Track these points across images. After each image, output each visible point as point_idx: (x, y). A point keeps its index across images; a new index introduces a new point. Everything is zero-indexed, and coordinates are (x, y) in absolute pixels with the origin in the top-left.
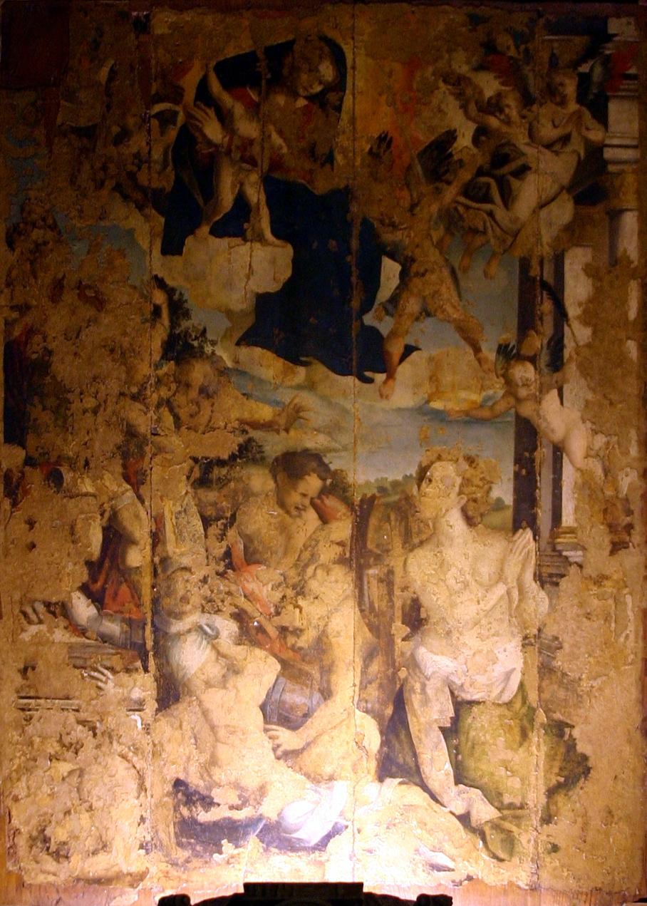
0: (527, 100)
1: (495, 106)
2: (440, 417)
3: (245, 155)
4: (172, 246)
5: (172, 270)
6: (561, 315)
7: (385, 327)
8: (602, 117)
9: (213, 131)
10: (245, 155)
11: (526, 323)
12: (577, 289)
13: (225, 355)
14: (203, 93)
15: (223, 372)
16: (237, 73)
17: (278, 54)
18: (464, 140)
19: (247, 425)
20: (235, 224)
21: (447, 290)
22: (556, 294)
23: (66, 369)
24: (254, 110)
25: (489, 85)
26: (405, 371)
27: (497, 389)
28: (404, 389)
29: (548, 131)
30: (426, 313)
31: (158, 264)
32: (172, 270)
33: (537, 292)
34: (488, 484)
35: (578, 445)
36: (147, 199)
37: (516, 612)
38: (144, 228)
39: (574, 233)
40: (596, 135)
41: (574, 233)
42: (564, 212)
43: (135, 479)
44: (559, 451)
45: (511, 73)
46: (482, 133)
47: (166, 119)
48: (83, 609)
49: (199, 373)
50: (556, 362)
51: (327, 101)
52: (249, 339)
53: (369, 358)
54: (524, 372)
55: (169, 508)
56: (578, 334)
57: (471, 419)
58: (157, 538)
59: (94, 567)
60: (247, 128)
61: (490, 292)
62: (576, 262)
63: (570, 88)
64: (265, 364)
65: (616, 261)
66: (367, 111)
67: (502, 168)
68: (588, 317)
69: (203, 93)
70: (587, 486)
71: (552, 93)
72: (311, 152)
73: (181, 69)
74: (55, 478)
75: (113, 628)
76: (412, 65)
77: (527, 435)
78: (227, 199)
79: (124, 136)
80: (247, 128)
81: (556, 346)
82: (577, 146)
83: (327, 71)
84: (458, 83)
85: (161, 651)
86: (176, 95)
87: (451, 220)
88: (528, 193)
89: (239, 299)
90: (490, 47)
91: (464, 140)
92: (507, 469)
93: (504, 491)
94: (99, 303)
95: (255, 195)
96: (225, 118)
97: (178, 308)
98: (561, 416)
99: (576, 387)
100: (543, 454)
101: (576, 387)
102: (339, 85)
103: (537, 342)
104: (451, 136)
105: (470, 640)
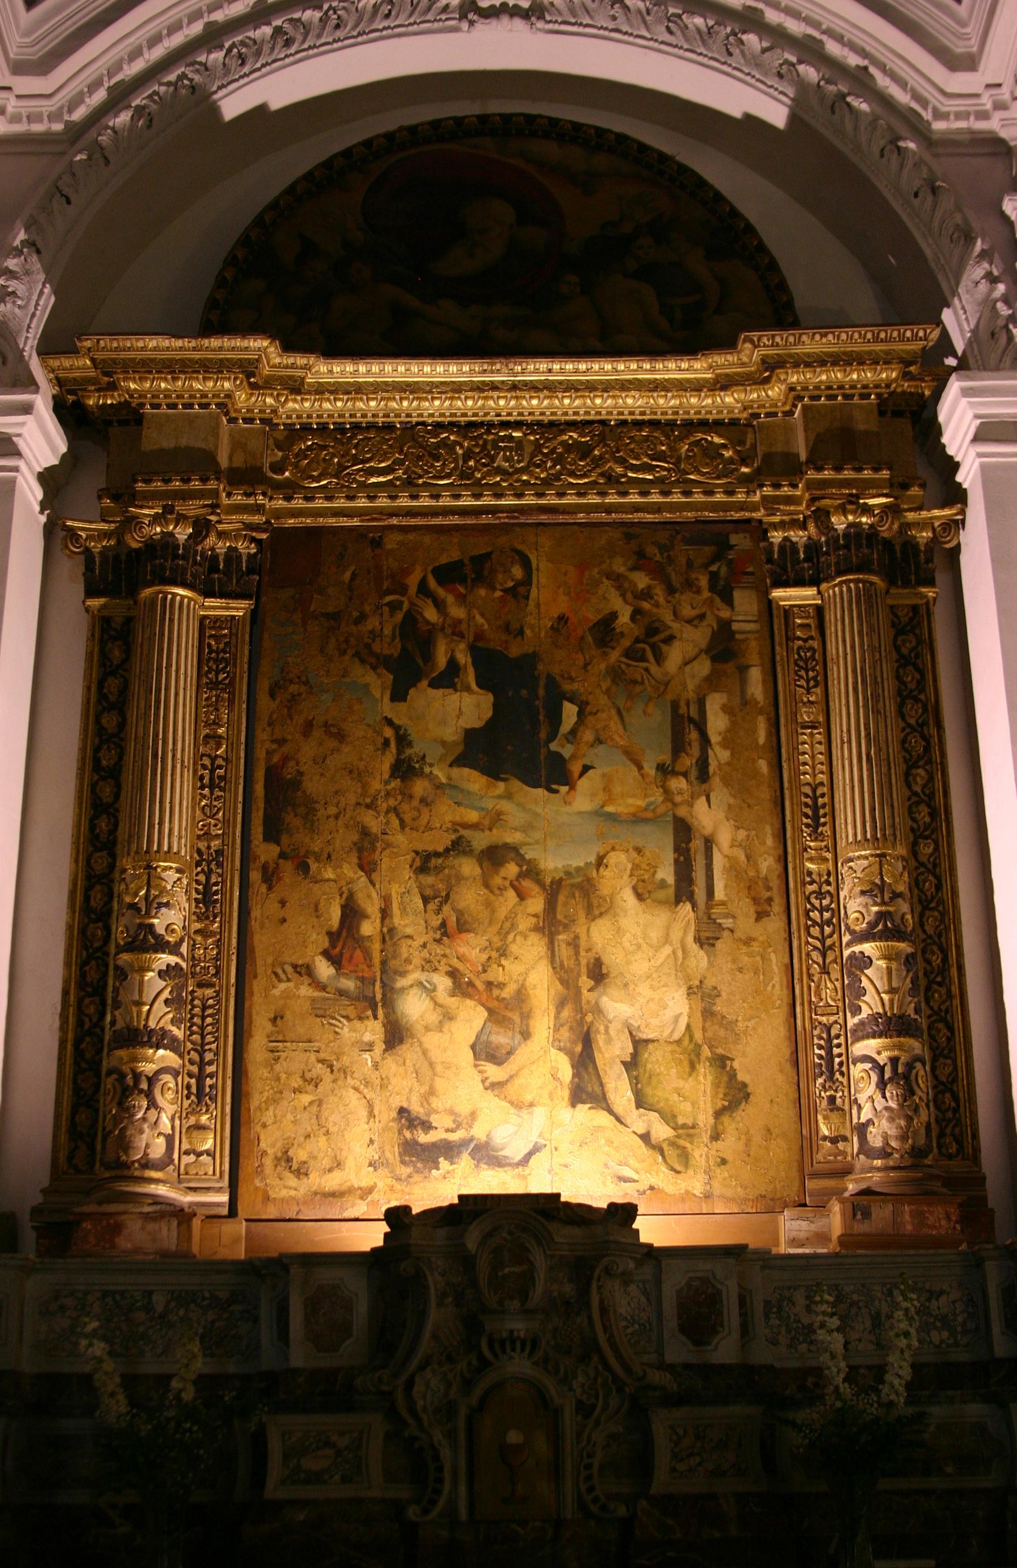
0: (671, 590)
1: (646, 594)
2: (612, 817)
3: (456, 631)
4: (399, 695)
5: (400, 714)
6: (705, 741)
7: (567, 751)
8: (729, 602)
9: (431, 614)
10: (456, 631)
11: (678, 747)
12: (717, 723)
13: (440, 774)
14: (423, 589)
15: (439, 786)
16: (449, 574)
17: (480, 561)
18: (624, 618)
19: (457, 826)
20: (448, 679)
21: (615, 725)
22: (701, 727)
23: (313, 785)
24: (462, 599)
25: (642, 580)
26: (584, 784)
27: (658, 796)
28: (584, 797)
29: (687, 612)
30: (599, 741)
31: (387, 708)
32: (400, 714)
33: (685, 726)
34: (653, 869)
35: (724, 837)
36: (378, 662)
37: (681, 968)
38: (378, 684)
39: (712, 682)
40: (725, 613)
41: (712, 682)
42: (703, 667)
43: (368, 868)
44: (709, 843)
45: (658, 572)
46: (637, 613)
47: (394, 607)
48: (324, 970)
49: (420, 787)
50: (703, 775)
51: (519, 592)
52: (460, 761)
53: (555, 775)
54: (678, 784)
55: (395, 890)
56: (719, 756)
57: (637, 819)
58: (385, 913)
59: (333, 937)
60: (457, 612)
61: (649, 725)
62: (714, 704)
63: (704, 582)
64: (473, 780)
65: (746, 702)
66: (548, 598)
67: (653, 638)
68: (725, 744)
69: (423, 589)
70: (733, 869)
71: (690, 585)
72: (507, 628)
73: (406, 572)
74: (303, 868)
75: (349, 984)
76: (582, 567)
77: (683, 831)
78: (442, 661)
79: (362, 618)
80: (457, 612)
81: (703, 765)
82: (711, 621)
83: (517, 572)
84: (618, 580)
85: (389, 1001)
86: (403, 590)
87: (616, 674)
88: (674, 656)
89: (452, 733)
90: (641, 554)
91: (624, 618)
92: (669, 857)
93: (666, 873)
94: (341, 737)
95: (463, 658)
96: (439, 605)
97: (403, 740)
98: (709, 816)
99: (720, 794)
100: (697, 844)
101: (720, 794)
102: (527, 581)
103: (687, 762)
104: (614, 616)
105: (644, 990)
